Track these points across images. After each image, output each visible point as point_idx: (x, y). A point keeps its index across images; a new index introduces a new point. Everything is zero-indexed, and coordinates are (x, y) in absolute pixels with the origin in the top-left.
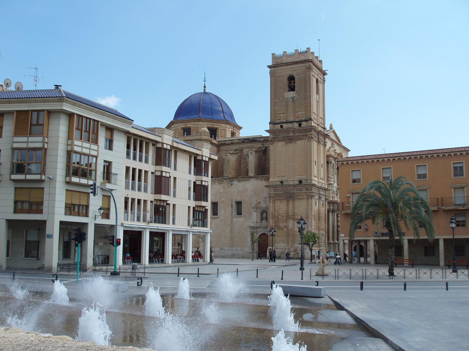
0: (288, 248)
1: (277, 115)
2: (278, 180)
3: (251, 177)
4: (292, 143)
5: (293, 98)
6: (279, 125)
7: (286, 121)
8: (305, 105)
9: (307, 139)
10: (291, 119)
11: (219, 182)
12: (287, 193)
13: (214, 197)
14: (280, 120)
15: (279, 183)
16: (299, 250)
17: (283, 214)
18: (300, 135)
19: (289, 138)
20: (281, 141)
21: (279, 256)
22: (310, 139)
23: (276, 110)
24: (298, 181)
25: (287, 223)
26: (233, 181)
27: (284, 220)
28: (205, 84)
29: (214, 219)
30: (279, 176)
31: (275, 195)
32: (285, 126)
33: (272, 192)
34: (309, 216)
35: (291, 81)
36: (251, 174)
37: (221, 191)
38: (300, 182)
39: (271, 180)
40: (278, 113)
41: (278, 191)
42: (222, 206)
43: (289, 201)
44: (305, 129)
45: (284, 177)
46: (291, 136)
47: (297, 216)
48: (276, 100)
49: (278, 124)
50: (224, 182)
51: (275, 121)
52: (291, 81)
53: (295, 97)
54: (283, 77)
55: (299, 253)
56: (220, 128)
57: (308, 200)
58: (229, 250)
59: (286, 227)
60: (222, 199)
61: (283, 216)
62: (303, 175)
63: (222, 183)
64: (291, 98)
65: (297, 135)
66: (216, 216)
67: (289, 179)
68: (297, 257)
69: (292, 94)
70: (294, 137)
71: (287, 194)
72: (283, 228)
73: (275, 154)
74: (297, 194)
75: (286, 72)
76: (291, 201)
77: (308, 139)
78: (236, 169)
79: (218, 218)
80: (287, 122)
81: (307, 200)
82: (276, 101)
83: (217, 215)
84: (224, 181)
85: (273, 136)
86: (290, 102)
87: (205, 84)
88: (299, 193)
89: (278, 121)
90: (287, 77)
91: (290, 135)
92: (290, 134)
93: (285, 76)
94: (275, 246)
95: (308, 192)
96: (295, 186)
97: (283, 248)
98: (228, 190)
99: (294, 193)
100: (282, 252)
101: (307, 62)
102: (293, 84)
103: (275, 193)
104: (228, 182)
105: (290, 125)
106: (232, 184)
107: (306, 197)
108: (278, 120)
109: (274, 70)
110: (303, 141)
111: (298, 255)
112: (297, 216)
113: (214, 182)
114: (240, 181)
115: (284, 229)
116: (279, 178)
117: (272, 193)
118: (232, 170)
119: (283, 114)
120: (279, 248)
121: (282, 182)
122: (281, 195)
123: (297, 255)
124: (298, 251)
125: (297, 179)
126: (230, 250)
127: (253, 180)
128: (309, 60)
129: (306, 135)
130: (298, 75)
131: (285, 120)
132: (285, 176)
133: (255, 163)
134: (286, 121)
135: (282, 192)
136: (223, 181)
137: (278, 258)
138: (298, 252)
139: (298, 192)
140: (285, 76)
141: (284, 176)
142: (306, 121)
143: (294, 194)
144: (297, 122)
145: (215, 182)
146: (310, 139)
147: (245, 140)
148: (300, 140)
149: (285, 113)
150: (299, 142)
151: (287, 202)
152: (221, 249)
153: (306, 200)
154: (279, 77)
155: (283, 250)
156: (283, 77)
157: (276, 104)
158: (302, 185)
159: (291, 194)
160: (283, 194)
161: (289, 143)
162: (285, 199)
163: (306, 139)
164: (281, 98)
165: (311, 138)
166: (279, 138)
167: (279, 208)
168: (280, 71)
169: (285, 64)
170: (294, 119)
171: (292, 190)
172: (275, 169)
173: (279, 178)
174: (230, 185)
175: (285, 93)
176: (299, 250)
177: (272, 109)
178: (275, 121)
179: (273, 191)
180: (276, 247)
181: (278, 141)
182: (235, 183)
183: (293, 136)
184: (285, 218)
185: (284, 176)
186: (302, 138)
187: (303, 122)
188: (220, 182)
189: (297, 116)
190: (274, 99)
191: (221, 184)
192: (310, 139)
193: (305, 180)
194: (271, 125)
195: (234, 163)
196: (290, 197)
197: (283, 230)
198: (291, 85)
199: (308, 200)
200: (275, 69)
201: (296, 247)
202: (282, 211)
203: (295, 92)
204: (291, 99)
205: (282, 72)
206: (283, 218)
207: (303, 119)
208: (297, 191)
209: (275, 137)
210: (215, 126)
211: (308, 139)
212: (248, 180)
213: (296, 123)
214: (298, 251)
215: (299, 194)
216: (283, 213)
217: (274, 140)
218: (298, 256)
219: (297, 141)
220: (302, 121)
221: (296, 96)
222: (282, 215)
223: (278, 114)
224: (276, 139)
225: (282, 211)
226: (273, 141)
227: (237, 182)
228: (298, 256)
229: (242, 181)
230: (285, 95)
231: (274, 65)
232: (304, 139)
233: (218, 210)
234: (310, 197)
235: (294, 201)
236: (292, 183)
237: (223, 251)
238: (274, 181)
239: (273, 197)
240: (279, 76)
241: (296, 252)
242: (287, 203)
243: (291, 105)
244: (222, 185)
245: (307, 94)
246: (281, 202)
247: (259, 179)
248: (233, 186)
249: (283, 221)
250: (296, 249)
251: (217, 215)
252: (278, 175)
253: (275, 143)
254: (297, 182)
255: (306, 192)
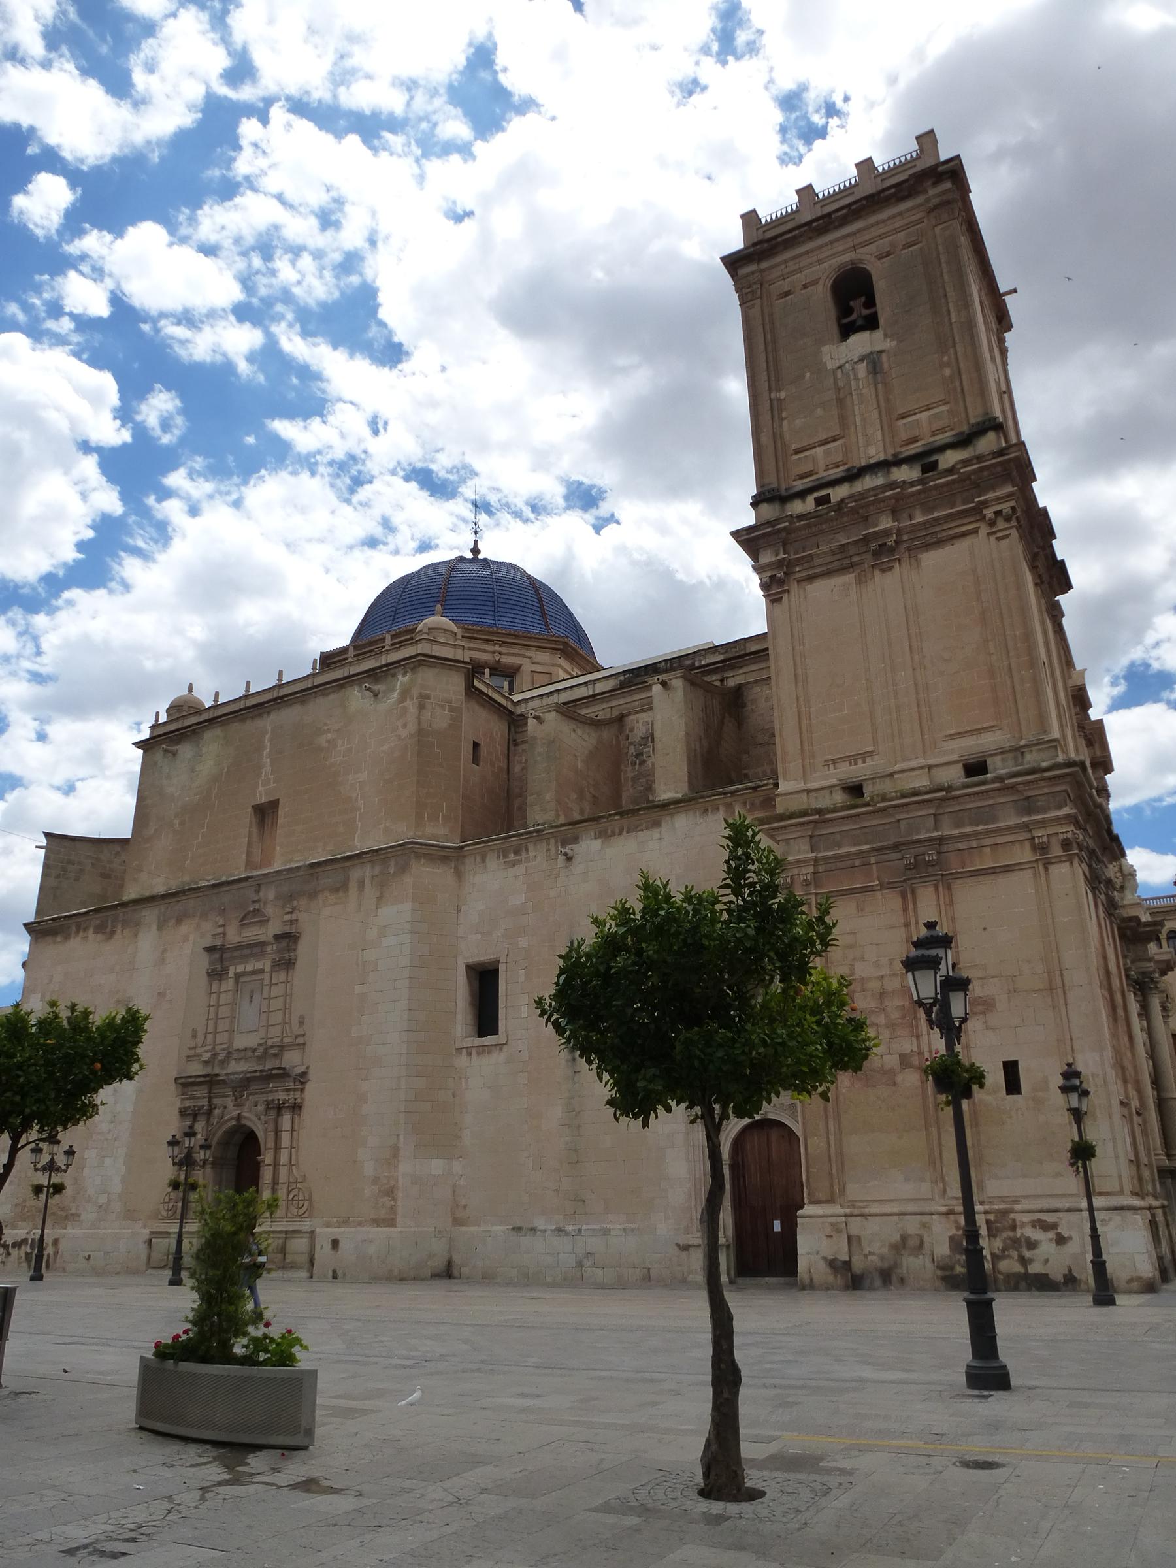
0: (944, 1209)
1: (795, 457)
2: (834, 781)
3: (665, 806)
4: (891, 568)
5: (873, 361)
6: (811, 499)
7: (843, 474)
8: (947, 372)
9: (984, 530)
10: (875, 453)
11: (505, 856)
12: (896, 847)
13: (479, 936)
14: (810, 474)
15: (839, 797)
16: (1026, 1218)
17: (882, 977)
18: (937, 519)
19: (874, 546)
20: (828, 573)
21: (886, 1265)
22: (1007, 525)
23: (787, 436)
24: (961, 765)
25: (918, 1037)
26: (575, 840)
27: (895, 1015)
28: (476, 542)
29: (478, 1054)
30: (834, 761)
31: (821, 868)
32: (838, 494)
33: (799, 852)
34: (1065, 973)
35: (852, 303)
36: (665, 792)
37: (518, 900)
38: (975, 768)
39: (784, 786)
40: (794, 447)
41: (840, 846)
42: (522, 979)
43: (913, 893)
44: (968, 476)
45: (864, 762)
46: (886, 533)
47: (982, 986)
48: (783, 395)
49: (802, 495)
50: (531, 855)
51: (783, 487)
52: (852, 303)
53: (881, 352)
54: (805, 287)
55: (1032, 1245)
56: (527, 667)
57: (1046, 869)
58: (559, 1230)
59: (911, 1066)
60: (523, 942)
61: (882, 995)
62: (985, 730)
63: (519, 862)
64: (862, 359)
65: (919, 518)
66: (489, 1040)
67: (898, 767)
68: (1018, 1268)
69: (861, 342)
70: (905, 537)
71: (897, 856)
72: (891, 1073)
73: (797, 648)
74: (961, 846)
75: (820, 262)
76: (931, 889)
77: (992, 523)
78: (594, 796)
79: (501, 1049)
80: (853, 475)
81: (1035, 875)
82: (779, 400)
83: (495, 1031)
84: (531, 847)
85: (777, 555)
86: (856, 378)
87: (476, 542)
88: (977, 834)
89: (799, 485)
90: (829, 284)
91: (877, 529)
92: (877, 525)
93: (815, 282)
94: (854, 1191)
95: (1043, 821)
96: (942, 796)
97: (911, 1208)
98: (553, 893)
99: (941, 840)
100: (904, 1238)
101: (930, 183)
102: (865, 312)
103: (816, 861)
104: (548, 850)
105: (869, 482)
106: (569, 859)
107: (1025, 854)
108: (802, 477)
109: (762, 271)
110: (963, 545)
111: (1027, 1254)
112: (982, 986)
113: (478, 859)
114: (613, 834)
115: (899, 1079)
116: (832, 771)
117: (798, 862)
118: (574, 796)
119: (825, 442)
120: (874, 1209)
121: (855, 790)
122: (857, 863)
123: (1015, 1254)
124: (1023, 1225)
125: (954, 757)
126: (567, 1234)
127: (681, 822)
128: (941, 169)
129: (978, 511)
130: (888, 254)
131: (842, 468)
132: (871, 753)
133: (687, 734)
134: (848, 470)
135: (868, 847)
136: (527, 850)
137: (878, 1282)
138: (1019, 1232)
139: (970, 829)
140: (815, 282)
141: (864, 756)
142: (963, 441)
143: (945, 848)
144: (909, 460)
145: (483, 860)
146: (1001, 524)
147: (638, 676)
148: (939, 543)
149: (834, 439)
150: (931, 559)
151: (904, 897)
152: (518, 1229)
153: (1027, 875)
154: (787, 294)
155: (912, 1226)
156: (805, 287)
157: (780, 411)
158: (993, 781)
159: (921, 850)
160: (873, 860)
161: (877, 573)
162: (882, 886)
163: (975, 531)
164: (808, 375)
165: (1008, 519)
166: (817, 562)
167: (851, 947)
168: (792, 266)
169: (814, 224)
170: (891, 451)
171: (930, 822)
172: (804, 722)
173: (832, 771)
174: (562, 858)
175: (825, 349)
176: (1026, 1218)
177: (765, 439)
178: (783, 487)
179: (808, 847)
180: (853, 1204)
181: (811, 579)
182: (589, 847)
183: (899, 532)
184: (898, 1002)
185: (864, 756)
186: (952, 532)
187: (949, 453)
188: (512, 857)
189: (904, 436)
190: (770, 390)
191: (514, 864)
192: (1001, 524)
193: (1010, 755)
194: (764, 507)
195: (580, 765)
196: (917, 866)
197: (895, 1084)
198: (853, 317)
199: (1046, 869)
200: (765, 265)
201: (1002, 1199)
202: (877, 964)
203: (878, 334)
204: (862, 369)
205: (800, 270)
206: (887, 1003)
207: (946, 437)
208: (958, 825)
209: (793, 557)
210: (505, 659)
211: (992, 523)
212: (657, 824)
213: (904, 467)
214: (1023, 1225)
215: (974, 844)
216: (885, 971)
217: (785, 573)
218: (1023, 1261)
219: (920, 556)
220: (942, 449)
221: (888, 344)
222: (874, 985)
223: (797, 452)
224: (800, 572)
225: (877, 964)
226: (781, 583)
227: (597, 844)
228: (1023, 1261)
229: (620, 833)
230: (826, 358)
231: (754, 245)
232: (964, 535)
233: (501, 1004)
234: (1056, 851)
235: (949, 889)
236: (921, 781)
237: (525, 1240)
238: (808, 791)
239: (807, 883)
240: (786, 289)
241: (1011, 1234)
242: (905, 910)
243: (864, 391)
244: (520, 869)
245: (953, 315)
246: (860, 908)
247: (718, 809)
248: (578, 867)
249: (891, 1026)
250: (1004, 1213)
251: (495, 1031)
252: (828, 757)
253: (794, 588)
254: (954, 775)
255: (1026, 827)
